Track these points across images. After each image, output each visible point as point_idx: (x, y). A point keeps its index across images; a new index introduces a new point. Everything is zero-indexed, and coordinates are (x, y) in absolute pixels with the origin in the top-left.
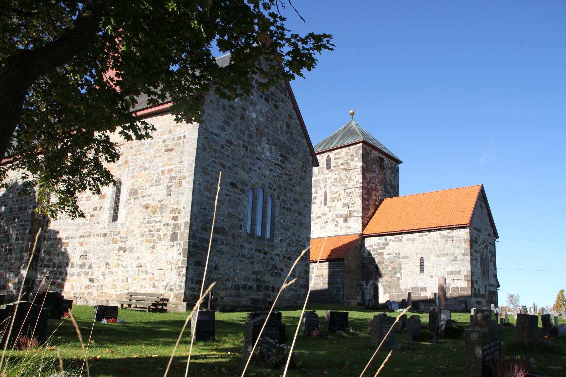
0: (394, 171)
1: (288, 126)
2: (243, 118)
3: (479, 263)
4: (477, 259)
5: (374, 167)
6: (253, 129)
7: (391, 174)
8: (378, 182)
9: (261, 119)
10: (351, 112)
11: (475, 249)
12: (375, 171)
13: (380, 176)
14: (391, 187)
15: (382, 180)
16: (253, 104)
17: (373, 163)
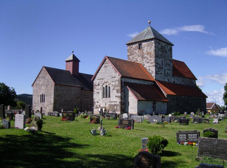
0: (150, 45)
1: (48, 80)
2: (39, 85)
3: (101, 94)
4: (98, 92)
5: (135, 51)
6: (41, 85)
7: (147, 48)
8: (138, 57)
9: (42, 83)
10: (149, 22)
11: (98, 88)
12: (136, 53)
13: (139, 53)
14: (148, 54)
15: (140, 55)
16: (41, 81)
17: (134, 50)
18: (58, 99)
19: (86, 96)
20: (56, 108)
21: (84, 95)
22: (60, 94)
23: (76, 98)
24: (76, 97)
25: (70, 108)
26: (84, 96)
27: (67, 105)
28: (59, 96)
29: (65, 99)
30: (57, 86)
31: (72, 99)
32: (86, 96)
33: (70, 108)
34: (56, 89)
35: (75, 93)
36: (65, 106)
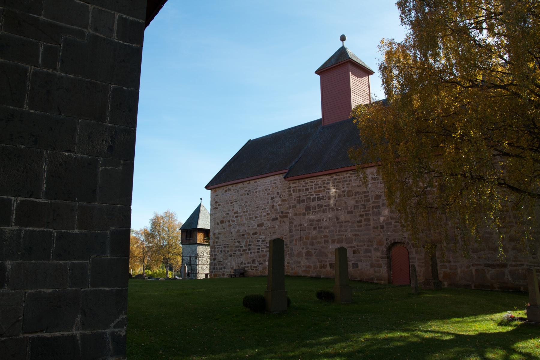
18: (219, 234)
19: (312, 204)
20: (216, 261)
21: (299, 202)
22: (224, 214)
23: (275, 219)
24: (273, 216)
25: (253, 261)
26: (298, 206)
27: (244, 250)
28: (222, 222)
29: (238, 231)
30: (217, 193)
31: (259, 225)
32: (312, 204)
33: (253, 261)
34: (216, 202)
35: (270, 201)
36: (238, 253)
